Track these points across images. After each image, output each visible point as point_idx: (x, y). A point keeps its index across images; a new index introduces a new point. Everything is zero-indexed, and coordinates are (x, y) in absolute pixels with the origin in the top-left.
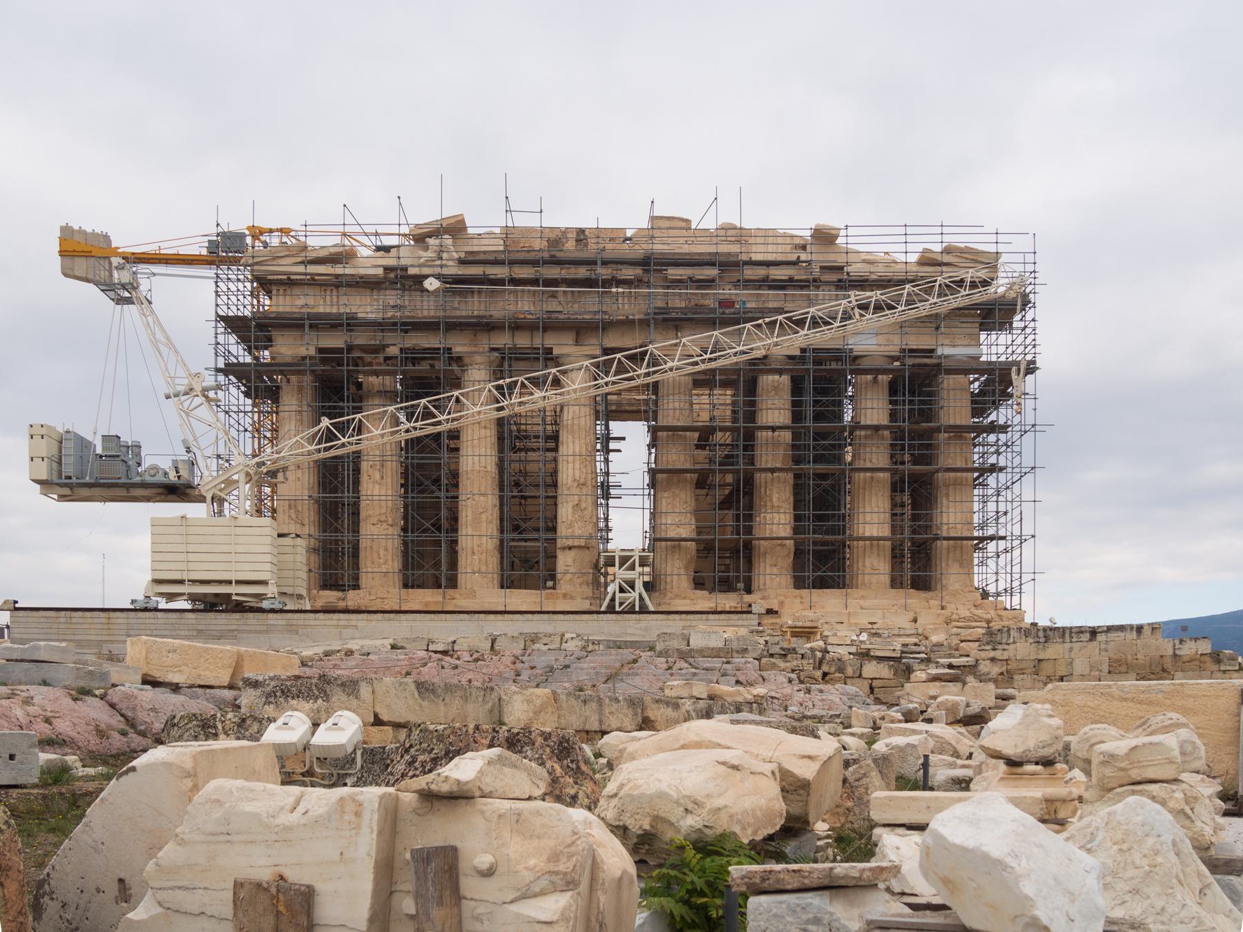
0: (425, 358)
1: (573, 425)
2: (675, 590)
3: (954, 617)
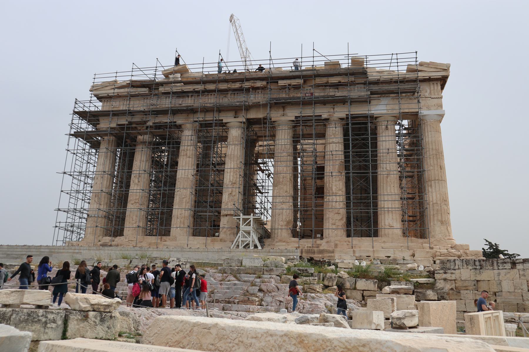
1: (231, 155)
3: (438, 254)
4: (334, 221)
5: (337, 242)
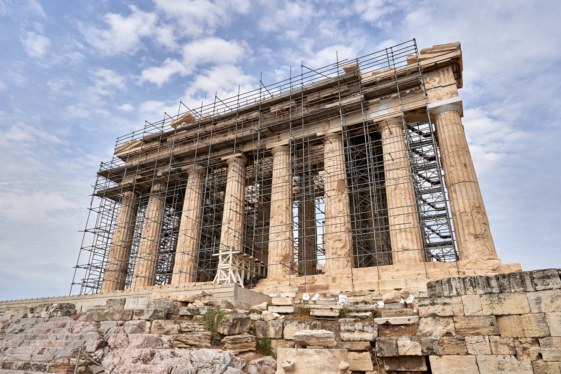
4: (334, 250)
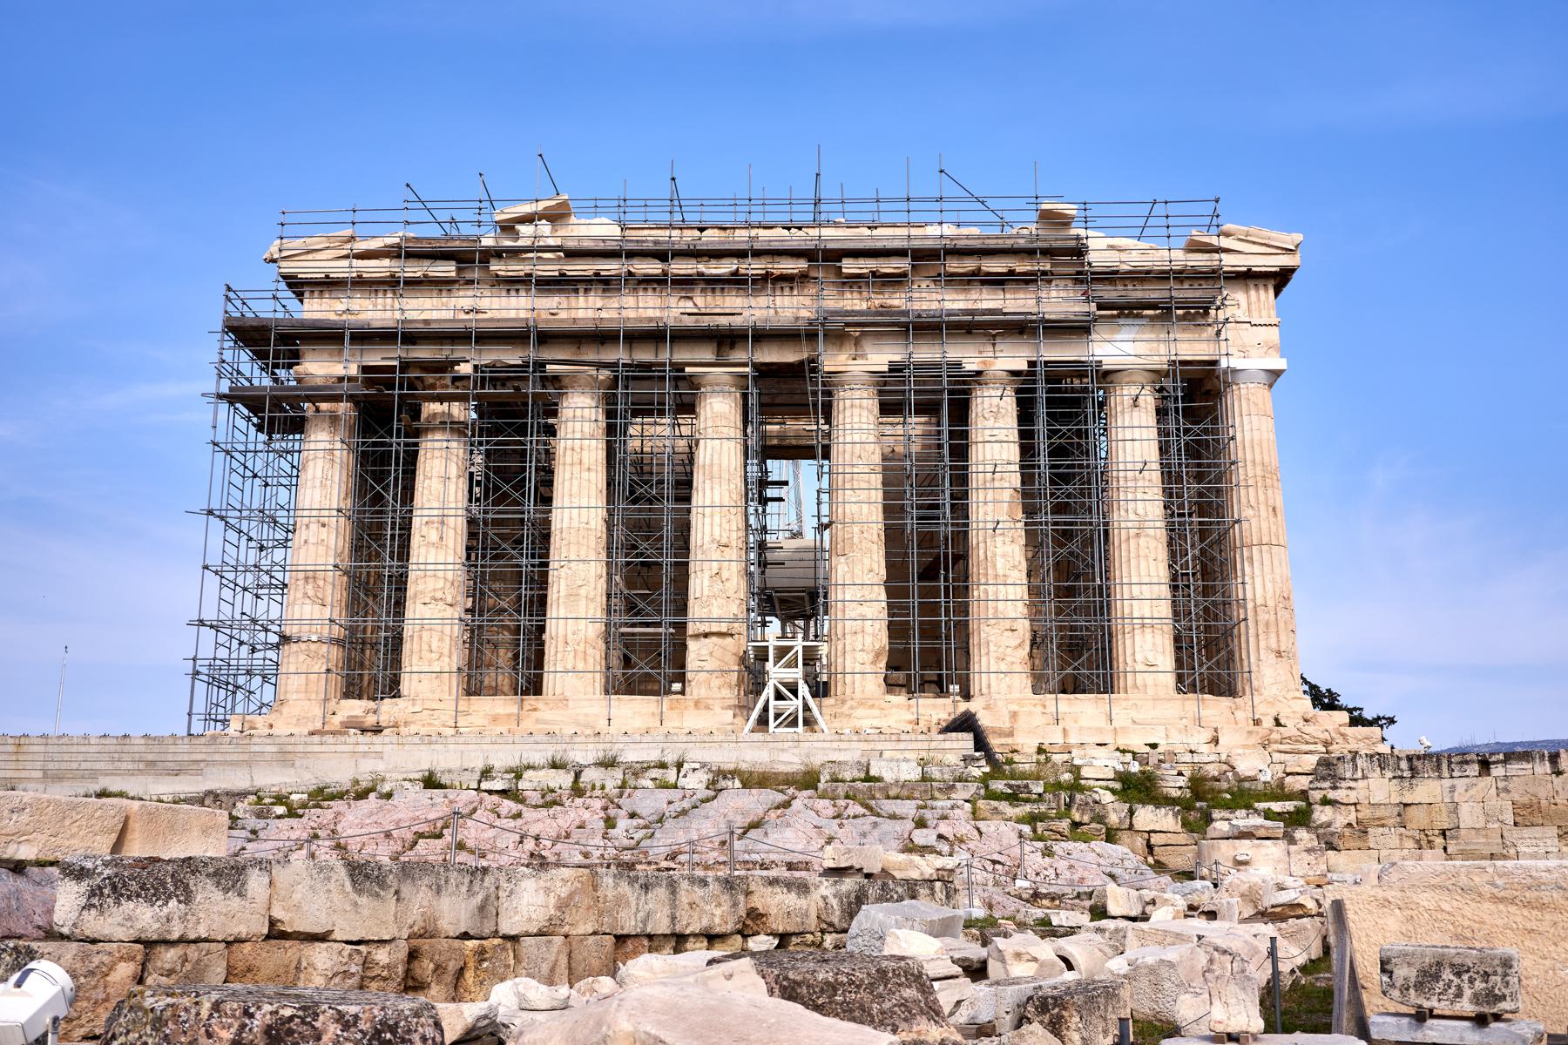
0: (509, 378)
1: (712, 465)
2: (858, 695)
5: (1014, 707)
